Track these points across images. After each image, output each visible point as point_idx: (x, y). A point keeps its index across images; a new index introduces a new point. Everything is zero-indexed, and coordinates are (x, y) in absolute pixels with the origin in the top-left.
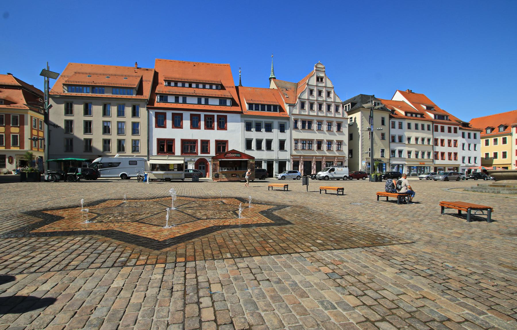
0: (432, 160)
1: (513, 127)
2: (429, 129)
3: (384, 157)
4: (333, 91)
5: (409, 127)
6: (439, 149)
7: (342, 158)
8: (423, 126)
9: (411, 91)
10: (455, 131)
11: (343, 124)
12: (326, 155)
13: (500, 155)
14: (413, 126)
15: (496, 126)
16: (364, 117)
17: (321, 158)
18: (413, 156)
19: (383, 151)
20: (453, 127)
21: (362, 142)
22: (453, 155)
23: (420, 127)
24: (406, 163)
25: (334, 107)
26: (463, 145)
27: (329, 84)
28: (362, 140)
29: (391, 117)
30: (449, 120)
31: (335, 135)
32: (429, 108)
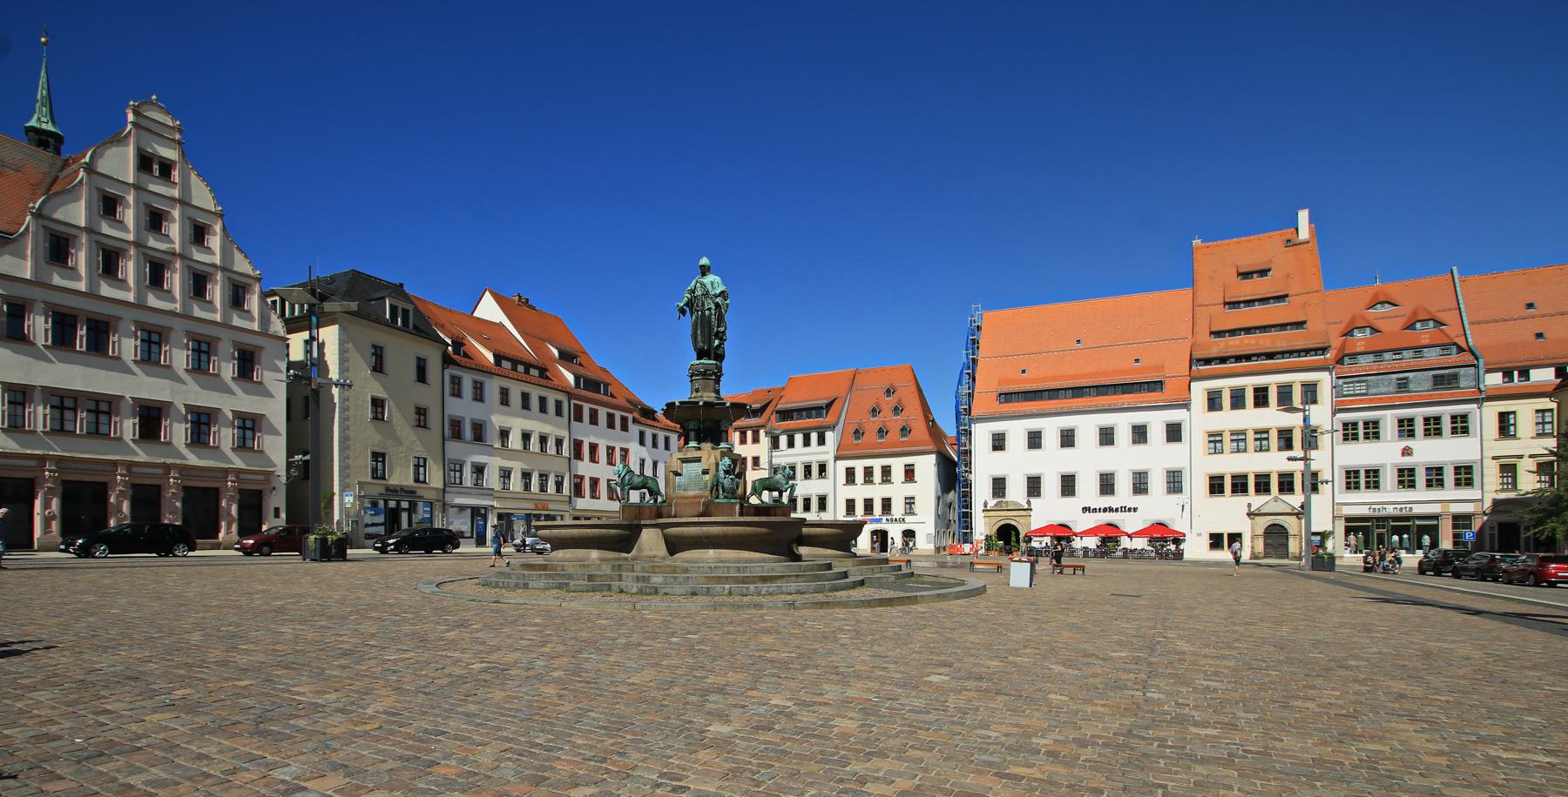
0: (567, 499)
2: (559, 413)
4: (218, 228)
5: (505, 398)
6: (585, 468)
8: (543, 400)
10: (624, 428)
11: (264, 357)
14: (515, 398)
16: (350, 346)
18: (516, 483)
19: (420, 465)
20: (618, 415)
21: (343, 429)
23: (535, 403)
25: (223, 289)
27: (203, 197)
28: (343, 421)
29: (447, 361)
30: (612, 396)
31: (232, 392)
32: (567, 357)
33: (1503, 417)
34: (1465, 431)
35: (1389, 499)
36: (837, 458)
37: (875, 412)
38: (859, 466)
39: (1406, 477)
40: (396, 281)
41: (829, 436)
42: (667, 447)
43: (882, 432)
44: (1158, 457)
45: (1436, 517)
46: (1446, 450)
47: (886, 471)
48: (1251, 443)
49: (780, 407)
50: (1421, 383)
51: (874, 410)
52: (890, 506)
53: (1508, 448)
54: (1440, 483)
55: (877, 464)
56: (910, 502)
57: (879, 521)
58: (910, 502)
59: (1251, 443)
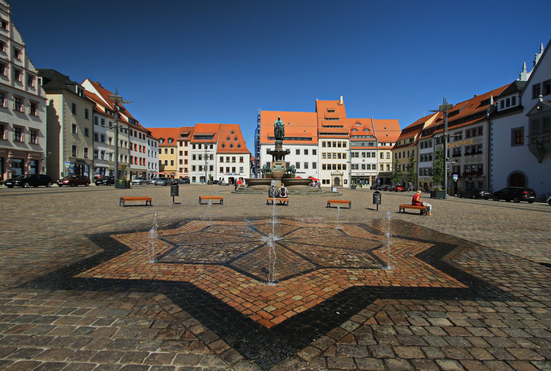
0: (128, 165)
1: (178, 141)
3: (87, 157)
7: (38, 155)
9: (100, 84)
10: (144, 139)
11: (39, 106)
12: (12, 148)
13: (169, 163)
15: (166, 138)
16: (66, 103)
17: (4, 152)
19: (86, 150)
21: (64, 136)
22: (142, 160)
24: (108, 166)
26: (149, 151)
28: (64, 132)
31: (28, 120)
33: (381, 153)
34: (374, 156)
35: (359, 172)
36: (217, 153)
37: (228, 139)
38: (225, 156)
39: (363, 167)
40: (66, 75)
41: (214, 146)
42: (156, 146)
43: (231, 146)
44: (310, 159)
45: (369, 176)
46: (370, 161)
47: (234, 159)
48: (332, 157)
49: (194, 134)
50: (366, 144)
51: (228, 138)
52: (235, 170)
53: (382, 161)
54: (370, 168)
55: (231, 156)
56: (241, 169)
57: (231, 174)
58: (241, 169)
59: (332, 157)
